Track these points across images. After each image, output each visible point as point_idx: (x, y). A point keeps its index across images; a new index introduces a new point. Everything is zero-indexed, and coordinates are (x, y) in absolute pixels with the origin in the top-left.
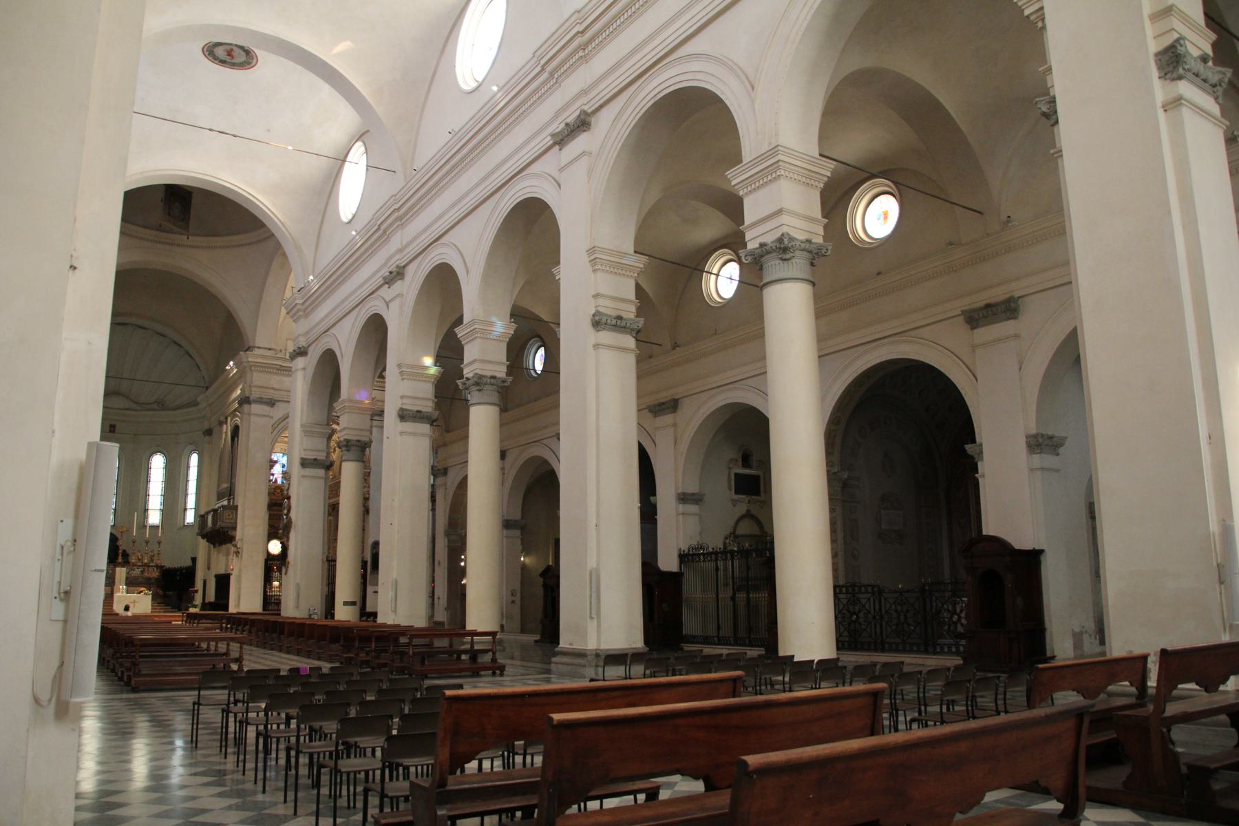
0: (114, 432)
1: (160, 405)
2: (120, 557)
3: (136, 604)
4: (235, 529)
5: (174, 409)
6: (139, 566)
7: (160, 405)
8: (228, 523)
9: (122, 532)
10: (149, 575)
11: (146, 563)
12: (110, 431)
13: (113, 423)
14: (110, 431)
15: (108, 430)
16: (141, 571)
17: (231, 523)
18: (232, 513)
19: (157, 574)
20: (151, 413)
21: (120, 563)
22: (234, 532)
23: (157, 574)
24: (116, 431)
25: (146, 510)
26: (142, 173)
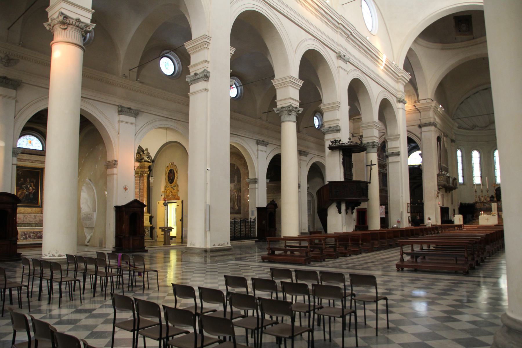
2: (495, 198)
3: (487, 220)
21: (495, 201)
26: (424, 19)
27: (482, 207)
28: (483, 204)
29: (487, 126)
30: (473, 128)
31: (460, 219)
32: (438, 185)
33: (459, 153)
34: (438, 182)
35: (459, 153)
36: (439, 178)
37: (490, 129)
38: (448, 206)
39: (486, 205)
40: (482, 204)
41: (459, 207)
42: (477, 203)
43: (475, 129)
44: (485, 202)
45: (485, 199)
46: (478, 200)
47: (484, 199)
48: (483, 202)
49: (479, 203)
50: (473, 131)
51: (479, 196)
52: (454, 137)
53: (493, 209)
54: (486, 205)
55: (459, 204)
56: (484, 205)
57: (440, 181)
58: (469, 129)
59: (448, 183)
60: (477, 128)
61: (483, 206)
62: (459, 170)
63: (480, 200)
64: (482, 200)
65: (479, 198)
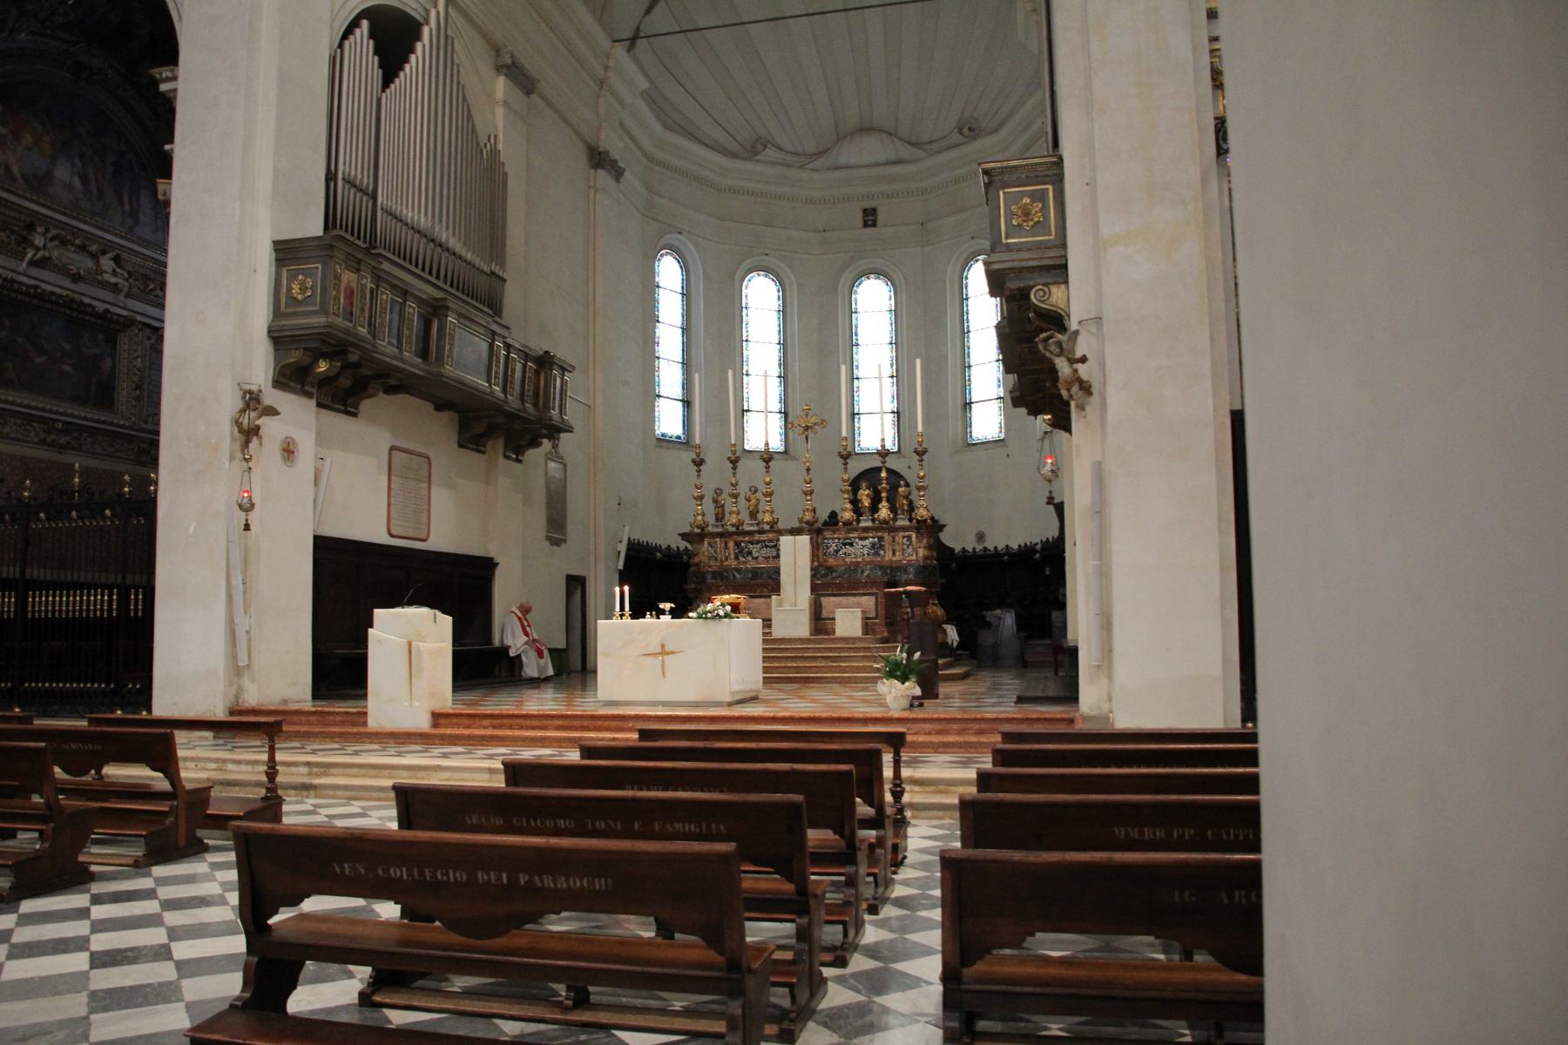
0: (874, 225)
1: (965, 130)
4: (1059, 271)
5: (996, 130)
6: (866, 529)
7: (965, 130)
8: (1019, 248)
9: (807, 428)
10: (898, 557)
11: (885, 522)
12: (866, 225)
13: (869, 204)
14: (866, 225)
15: (860, 224)
16: (873, 545)
17: (1039, 246)
18: (1041, 197)
19: (922, 552)
20: (952, 154)
22: (1057, 294)
23: (922, 552)
24: (879, 222)
25: (967, 405)
27: (732, 563)
28: (737, 544)
29: (821, 154)
30: (755, 148)
31: (410, 644)
32: (279, 339)
33: (669, 272)
34: (277, 313)
35: (669, 272)
36: (292, 277)
37: (838, 168)
38: (492, 552)
39: (755, 549)
40: (731, 544)
41: (621, 567)
42: (696, 536)
43: (758, 157)
44: (751, 533)
45: (753, 514)
46: (711, 519)
47: (745, 516)
48: (739, 532)
49: (714, 535)
50: (750, 166)
51: (719, 492)
52: (613, 144)
53: (785, 578)
54: (755, 549)
55: (623, 548)
56: (741, 552)
57: (292, 300)
58: (734, 155)
59: (424, 353)
60: (770, 153)
61: (737, 558)
62: (663, 365)
63: (720, 517)
64: (734, 519)
65: (715, 501)
